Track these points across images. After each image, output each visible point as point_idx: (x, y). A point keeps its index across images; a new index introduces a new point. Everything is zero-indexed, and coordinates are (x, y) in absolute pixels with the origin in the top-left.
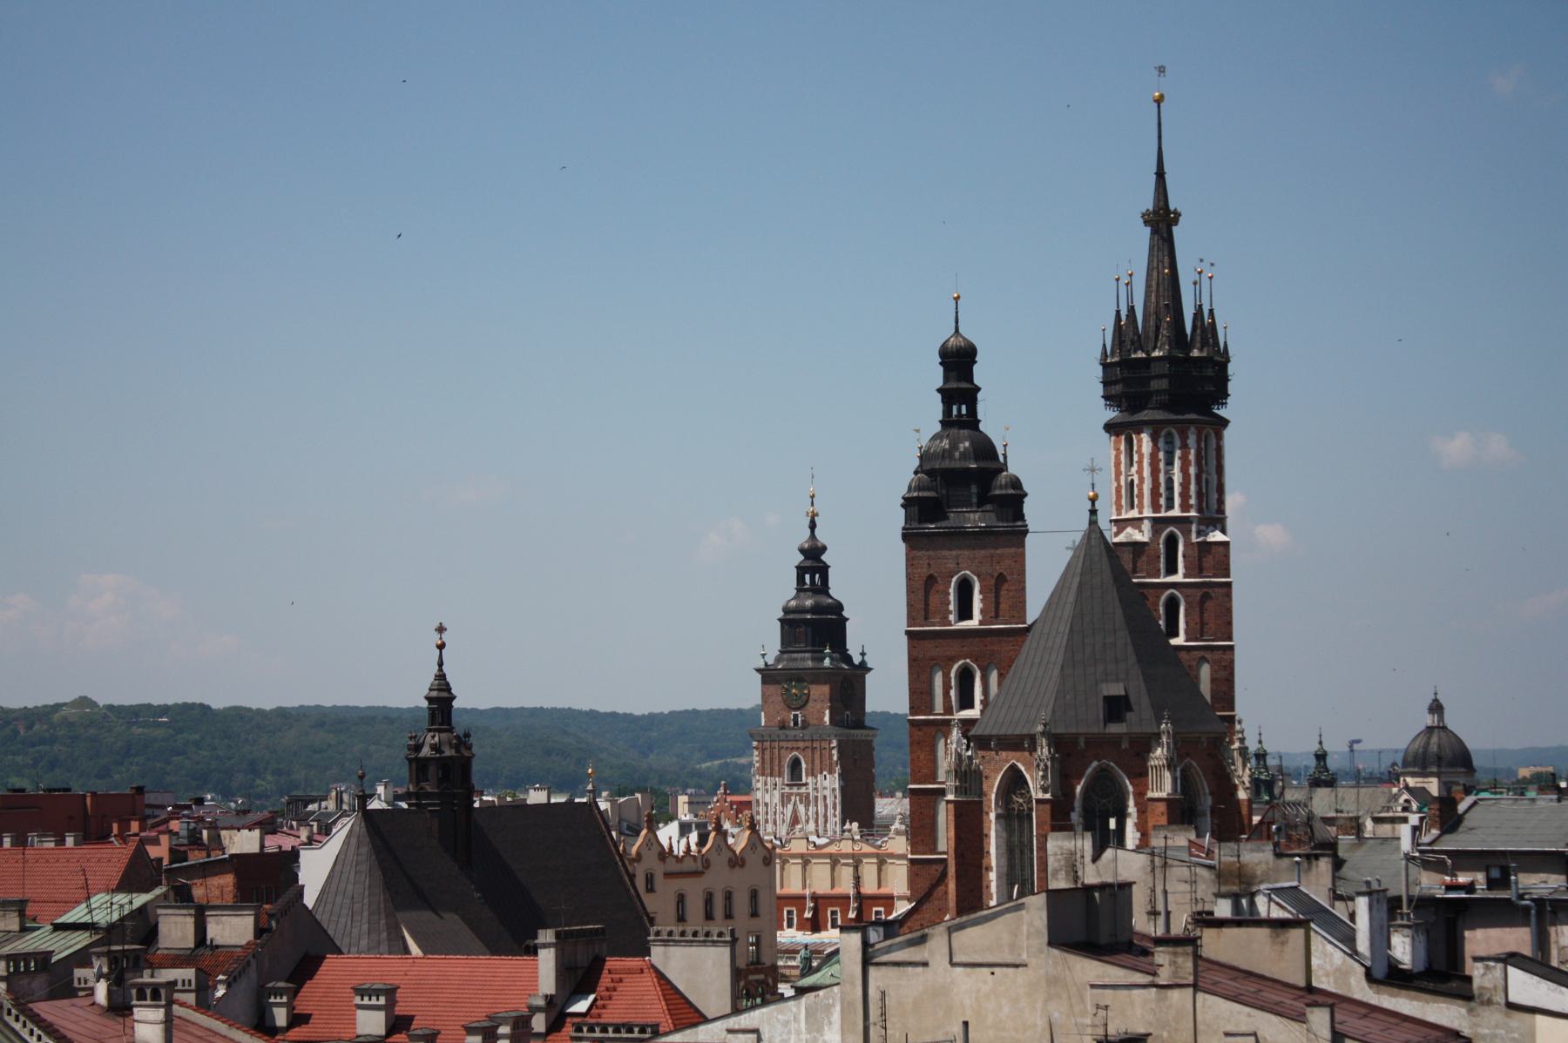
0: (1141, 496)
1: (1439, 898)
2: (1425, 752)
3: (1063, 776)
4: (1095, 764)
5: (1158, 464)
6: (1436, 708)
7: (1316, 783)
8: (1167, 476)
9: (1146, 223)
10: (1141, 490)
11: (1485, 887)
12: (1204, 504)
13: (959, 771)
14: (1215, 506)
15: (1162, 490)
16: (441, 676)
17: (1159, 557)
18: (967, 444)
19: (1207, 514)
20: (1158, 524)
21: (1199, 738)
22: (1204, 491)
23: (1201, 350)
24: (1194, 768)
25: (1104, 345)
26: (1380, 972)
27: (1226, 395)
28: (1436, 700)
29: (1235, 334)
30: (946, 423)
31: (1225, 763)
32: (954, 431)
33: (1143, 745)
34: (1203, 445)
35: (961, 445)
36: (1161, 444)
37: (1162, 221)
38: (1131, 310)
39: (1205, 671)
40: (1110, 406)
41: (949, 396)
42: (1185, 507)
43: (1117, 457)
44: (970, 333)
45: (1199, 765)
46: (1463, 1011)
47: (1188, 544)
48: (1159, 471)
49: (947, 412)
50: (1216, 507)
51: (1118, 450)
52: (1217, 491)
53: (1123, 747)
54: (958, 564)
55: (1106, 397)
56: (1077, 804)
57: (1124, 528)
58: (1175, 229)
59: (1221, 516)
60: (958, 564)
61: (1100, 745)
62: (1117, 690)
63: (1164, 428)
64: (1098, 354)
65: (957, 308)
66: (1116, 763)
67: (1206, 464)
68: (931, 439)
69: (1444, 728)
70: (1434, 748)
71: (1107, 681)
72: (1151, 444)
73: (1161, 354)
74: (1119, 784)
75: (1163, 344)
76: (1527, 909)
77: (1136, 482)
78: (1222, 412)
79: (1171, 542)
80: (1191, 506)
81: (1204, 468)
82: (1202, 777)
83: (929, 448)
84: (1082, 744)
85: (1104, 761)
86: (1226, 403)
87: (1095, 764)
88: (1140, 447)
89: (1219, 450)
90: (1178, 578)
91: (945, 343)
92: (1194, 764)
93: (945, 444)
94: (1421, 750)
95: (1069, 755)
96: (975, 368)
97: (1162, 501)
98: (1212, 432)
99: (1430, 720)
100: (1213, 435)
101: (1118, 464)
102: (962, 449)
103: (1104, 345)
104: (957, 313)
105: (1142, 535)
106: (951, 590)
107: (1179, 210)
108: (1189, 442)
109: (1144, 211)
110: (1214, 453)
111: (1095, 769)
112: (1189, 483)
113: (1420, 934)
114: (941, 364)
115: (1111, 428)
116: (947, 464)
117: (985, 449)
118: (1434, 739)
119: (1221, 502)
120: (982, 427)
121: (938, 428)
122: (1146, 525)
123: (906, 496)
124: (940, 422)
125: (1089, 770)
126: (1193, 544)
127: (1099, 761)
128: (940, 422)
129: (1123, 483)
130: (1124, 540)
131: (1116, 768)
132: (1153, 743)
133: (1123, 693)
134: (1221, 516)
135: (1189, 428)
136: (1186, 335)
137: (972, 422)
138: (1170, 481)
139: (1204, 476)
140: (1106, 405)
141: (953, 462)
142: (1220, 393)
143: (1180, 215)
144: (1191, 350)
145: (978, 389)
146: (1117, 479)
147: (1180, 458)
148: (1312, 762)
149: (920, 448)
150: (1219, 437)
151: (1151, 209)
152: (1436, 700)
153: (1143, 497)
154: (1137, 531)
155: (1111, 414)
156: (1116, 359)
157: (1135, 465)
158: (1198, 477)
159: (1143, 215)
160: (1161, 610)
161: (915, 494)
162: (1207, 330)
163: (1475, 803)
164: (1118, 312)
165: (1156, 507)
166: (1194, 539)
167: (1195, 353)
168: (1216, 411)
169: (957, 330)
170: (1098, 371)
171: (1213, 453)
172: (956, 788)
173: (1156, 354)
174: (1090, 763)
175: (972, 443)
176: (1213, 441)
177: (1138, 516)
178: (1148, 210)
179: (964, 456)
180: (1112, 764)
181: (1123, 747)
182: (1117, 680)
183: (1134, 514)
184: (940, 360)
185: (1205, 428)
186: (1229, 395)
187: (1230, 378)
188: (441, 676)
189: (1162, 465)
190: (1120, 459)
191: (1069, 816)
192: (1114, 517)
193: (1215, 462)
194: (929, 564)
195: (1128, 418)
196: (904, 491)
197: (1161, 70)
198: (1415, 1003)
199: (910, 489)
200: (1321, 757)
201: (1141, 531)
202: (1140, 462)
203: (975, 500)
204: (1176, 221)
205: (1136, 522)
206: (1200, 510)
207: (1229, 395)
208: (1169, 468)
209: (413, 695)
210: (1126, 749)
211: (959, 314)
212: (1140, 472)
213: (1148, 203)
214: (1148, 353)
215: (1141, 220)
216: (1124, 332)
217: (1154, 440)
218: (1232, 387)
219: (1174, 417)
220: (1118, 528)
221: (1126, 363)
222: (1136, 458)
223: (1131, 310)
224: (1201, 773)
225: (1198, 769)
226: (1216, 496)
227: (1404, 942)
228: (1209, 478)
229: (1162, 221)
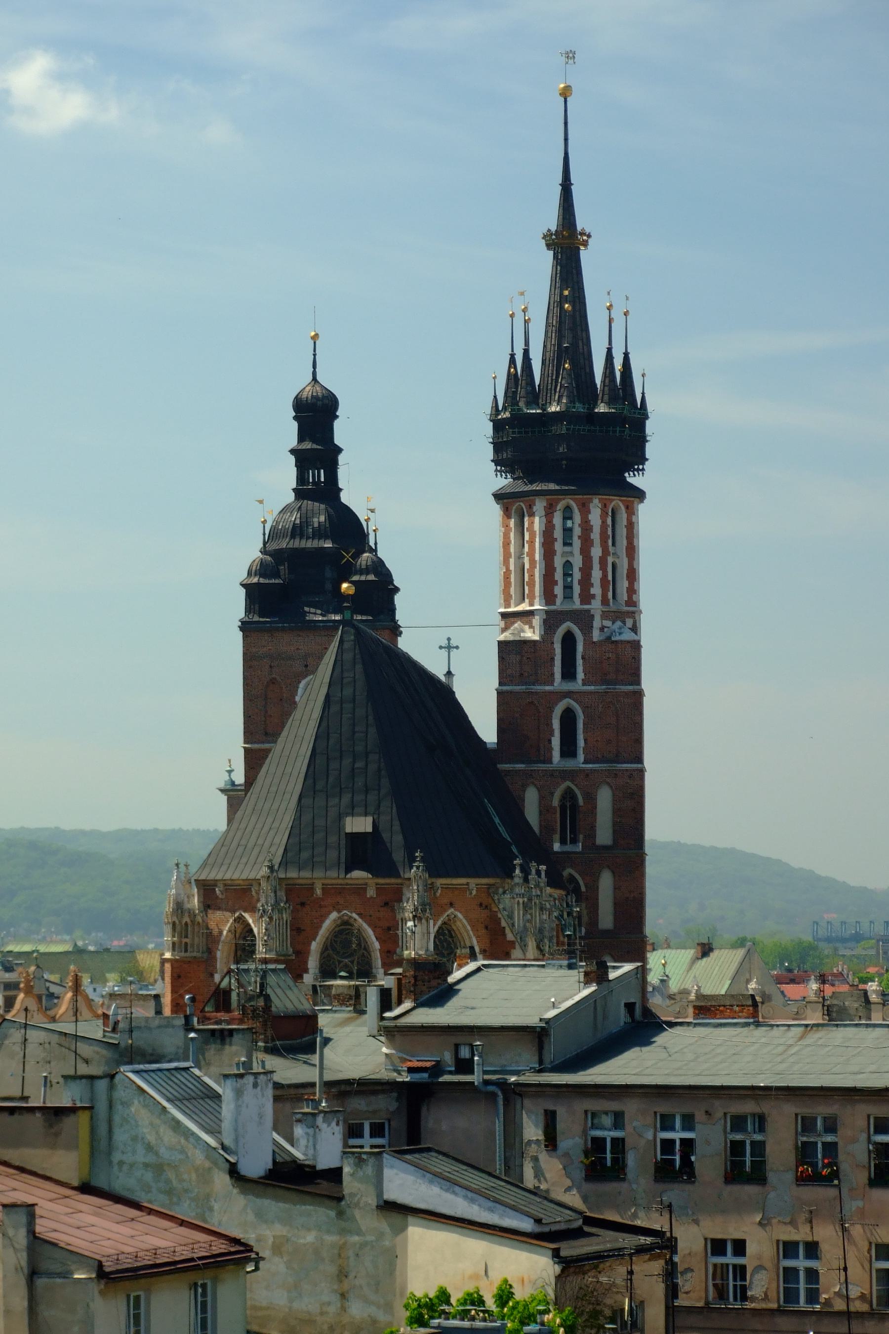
0: (532, 584)
1: (399, 1082)
4: (334, 915)
5: (553, 544)
8: (564, 560)
9: (549, 246)
10: (532, 576)
11: (453, 1069)
12: (610, 594)
13: (177, 922)
14: (623, 596)
15: (559, 575)
17: (553, 659)
18: (322, 519)
19: (612, 607)
20: (551, 621)
21: (468, 884)
22: (610, 578)
23: (609, 404)
24: (461, 921)
25: (495, 397)
27: (643, 459)
30: (299, 493)
31: (500, 916)
32: (308, 504)
34: (609, 521)
35: (316, 520)
36: (557, 519)
39: (604, 799)
40: (501, 471)
42: (586, 597)
43: (506, 536)
44: (329, 381)
45: (466, 917)
47: (589, 643)
49: (301, 478)
52: (628, 577)
53: (368, 896)
54: (306, 666)
55: (496, 462)
57: (514, 623)
58: (584, 254)
59: (632, 609)
60: (306, 666)
62: (361, 824)
63: (560, 500)
65: (315, 350)
66: (360, 915)
67: (614, 544)
68: (281, 512)
72: (544, 519)
73: (558, 409)
74: (364, 939)
75: (560, 397)
76: (494, 1095)
77: (527, 566)
78: (634, 480)
79: (569, 641)
80: (593, 596)
81: (611, 549)
82: (471, 933)
84: (319, 892)
85: (345, 911)
86: (643, 469)
87: (334, 915)
88: (532, 523)
89: (631, 527)
90: (578, 685)
91: (297, 395)
92: (460, 915)
93: (295, 517)
95: (303, 904)
96: (336, 424)
97: (558, 590)
98: (621, 504)
100: (623, 508)
101: (506, 544)
102: (316, 525)
103: (495, 397)
104: (315, 355)
105: (531, 633)
107: (587, 231)
108: (590, 517)
109: (545, 231)
110: (625, 531)
111: (335, 920)
112: (591, 568)
113: (334, 1124)
114: (295, 418)
115: (499, 497)
116: (297, 543)
119: (632, 591)
120: (344, 498)
121: (291, 497)
122: (537, 621)
123: (244, 582)
124: (294, 490)
126: (594, 643)
127: (339, 911)
128: (294, 490)
129: (512, 567)
130: (511, 638)
131: (360, 920)
132: (405, 891)
133: (369, 829)
134: (632, 609)
135: (591, 500)
136: (595, 385)
138: (568, 565)
139: (610, 560)
140: (496, 470)
141: (303, 542)
143: (589, 236)
144: (595, 405)
145: (339, 450)
147: (579, 537)
149: (264, 522)
150: (631, 511)
151: (554, 228)
153: (534, 585)
154: (527, 627)
155: (502, 482)
156: (507, 415)
157: (526, 546)
158: (603, 562)
159: (544, 237)
160: (556, 724)
163: (478, 970)
165: (549, 596)
166: (596, 636)
167: (602, 408)
168: (629, 480)
169: (314, 379)
170: (488, 429)
171: (622, 532)
172: (174, 944)
173: (554, 408)
174: (330, 913)
175: (329, 517)
177: (528, 608)
178: (549, 230)
179: (319, 534)
180: (354, 915)
181: (368, 896)
182: (366, 815)
183: (524, 607)
184: (294, 414)
185: (614, 500)
186: (647, 460)
187: (648, 438)
189: (558, 546)
190: (509, 538)
192: (502, 610)
193: (625, 542)
194: (271, 667)
195: (522, 487)
196: (243, 575)
198: (281, 1205)
199: (249, 573)
201: (531, 627)
202: (532, 542)
204: (585, 244)
205: (527, 615)
206: (605, 601)
207: (647, 460)
208: (567, 549)
210: (372, 898)
211: (317, 357)
213: (551, 221)
214: (544, 410)
218: (650, 450)
219: (557, 488)
220: (506, 623)
222: (527, 537)
223: (526, 352)
224: (469, 928)
225: (464, 921)
226: (626, 584)
227: (307, 1134)
228: (617, 561)
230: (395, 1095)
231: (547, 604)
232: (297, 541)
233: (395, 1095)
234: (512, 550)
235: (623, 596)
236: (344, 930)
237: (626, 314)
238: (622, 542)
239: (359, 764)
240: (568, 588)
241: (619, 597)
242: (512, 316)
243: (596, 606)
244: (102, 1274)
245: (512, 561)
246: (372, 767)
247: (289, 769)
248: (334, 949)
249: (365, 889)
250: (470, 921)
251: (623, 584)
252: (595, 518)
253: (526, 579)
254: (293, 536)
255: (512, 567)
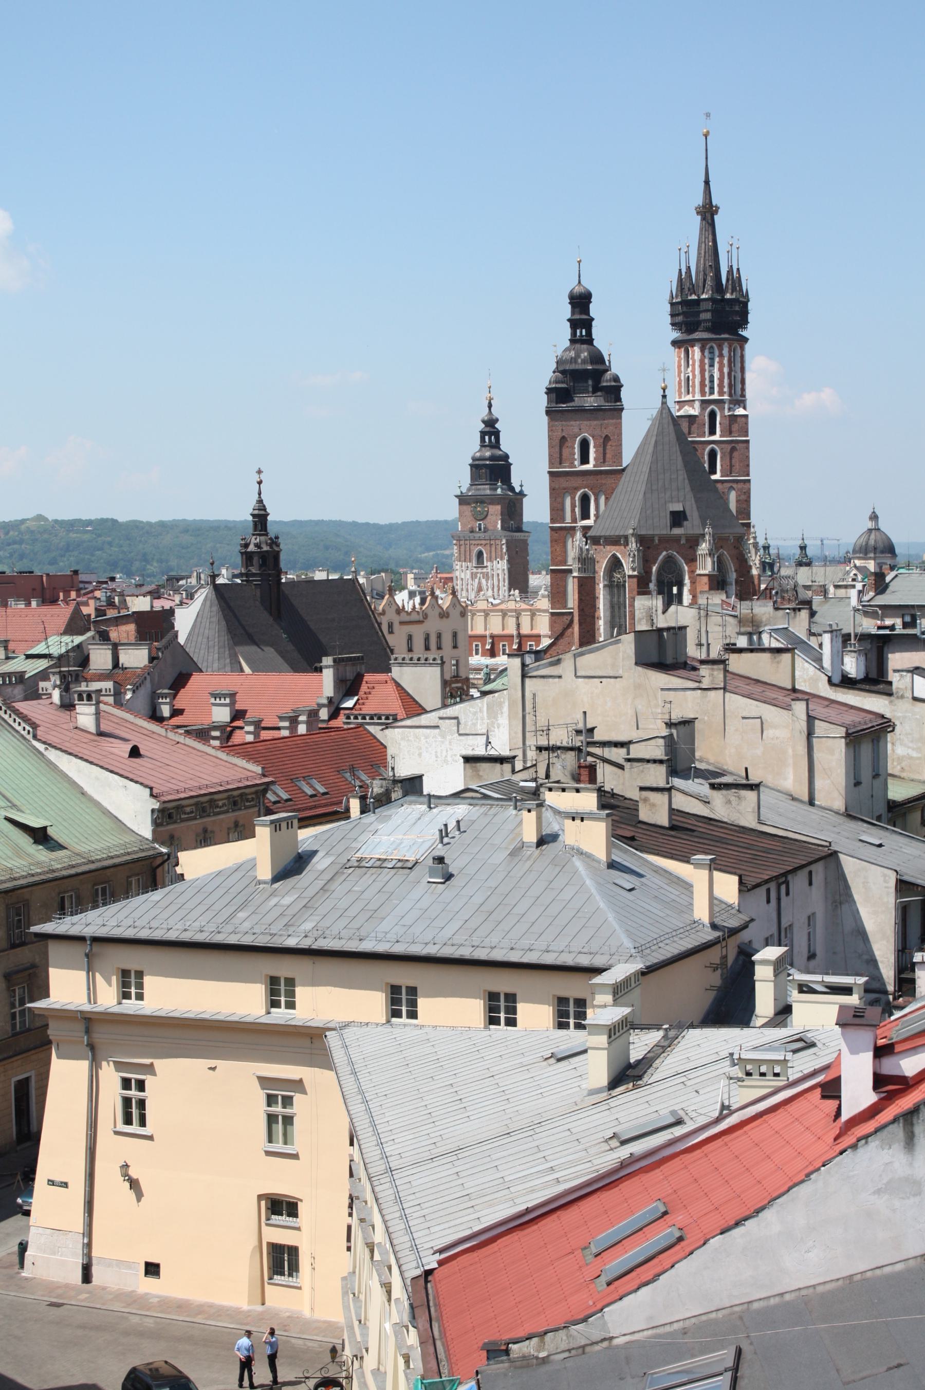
0: (694, 386)
2: (867, 544)
3: (646, 560)
4: (664, 553)
6: (874, 517)
7: (800, 564)
9: (698, 213)
10: (694, 382)
14: (739, 392)
15: (707, 382)
16: (260, 501)
17: (705, 424)
18: (586, 354)
19: (734, 398)
20: (704, 403)
23: (732, 294)
26: (837, 679)
27: (747, 322)
28: (874, 512)
29: (751, 284)
30: (573, 341)
32: (578, 346)
33: (694, 542)
37: (708, 212)
38: (689, 268)
39: (733, 496)
41: (574, 324)
42: (721, 393)
43: (679, 362)
44: (589, 284)
46: (887, 702)
47: (723, 416)
48: (705, 370)
49: (574, 334)
50: (740, 393)
51: (679, 357)
55: (672, 324)
56: (654, 578)
58: (716, 217)
61: (668, 541)
62: (678, 507)
64: (668, 297)
66: (677, 552)
69: (879, 529)
70: (872, 542)
71: (672, 502)
72: (700, 353)
75: (708, 291)
77: (691, 378)
78: (744, 333)
79: (712, 415)
80: (725, 393)
83: (562, 357)
84: (657, 541)
87: (664, 553)
88: (693, 355)
89: (742, 357)
90: (716, 437)
93: (573, 354)
94: (864, 544)
95: (649, 548)
96: (591, 306)
97: (707, 389)
99: (870, 525)
101: (679, 366)
102: (583, 357)
105: (694, 411)
106: (576, 446)
109: (697, 205)
112: (724, 378)
114: (570, 303)
115: (676, 343)
116: (573, 367)
117: (597, 358)
118: (873, 536)
119: (743, 389)
120: (595, 343)
121: (568, 344)
122: (697, 405)
125: (661, 557)
129: (682, 378)
130: (683, 414)
132: (700, 540)
133: (682, 509)
135: (724, 344)
137: (589, 340)
138: (712, 377)
139: (733, 374)
142: (743, 319)
145: (593, 319)
146: (679, 375)
148: (798, 551)
149: (557, 357)
150: (742, 349)
152: (874, 512)
155: (676, 335)
156: (679, 300)
157: (690, 367)
160: (706, 458)
161: (554, 386)
162: (736, 282)
163: (896, 576)
164: (680, 270)
165: (703, 393)
167: (728, 296)
168: (740, 333)
169: (579, 282)
171: (738, 359)
173: (704, 296)
174: (662, 552)
175: (589, 354)
176: (739, 351)
177: (692, 399)
179: (584, 362)
180: (675, 553)
182: (679, 501)
183: (689, 397)
188: (260, 501)
189: (707, 367)
191: (648, 585)
192: (677, 400)
193: (739, 365)
196: (546, 384)
197: (708, 115)
198: (858, 698)
200: (803, 548)
201: (693, 408)
202: (694, 365)
203: (591, 389)
204: (716, 212)
205: (691, 402)
206: (730, 395)
208: (712, 368)
209: (244, 514)
212: (693, 371)
213: (699, 200)
214: (698, 296)
215: (695, 212)
216: (684, 283)
217: (702, 351)
218: (750, 317)
221: (685, 303)
223: (689, 268)
229: (708, 212)
230: (869, 641)
231: (702, 396)
232: (574, 365)
233: (869, 641)
234: (683, 369)
235: (739, 392)
236: (669, 560)
237: (738, 248)
238: (738, 365)
239: (674, 476)
240: (712, 388)
241: (737, 392)
242: (680, 249)
243: (726, 397)
244: (848, 735)
245: (682, 375)
246: (680, 478)
247: (637, 479)
248: (663, 570)
249: (680, 540)
250: (730, 556)
251: (739, 386)
252: (725, 351)
253: (691, 384)
254: (571, 362)
255: (682, 378)
